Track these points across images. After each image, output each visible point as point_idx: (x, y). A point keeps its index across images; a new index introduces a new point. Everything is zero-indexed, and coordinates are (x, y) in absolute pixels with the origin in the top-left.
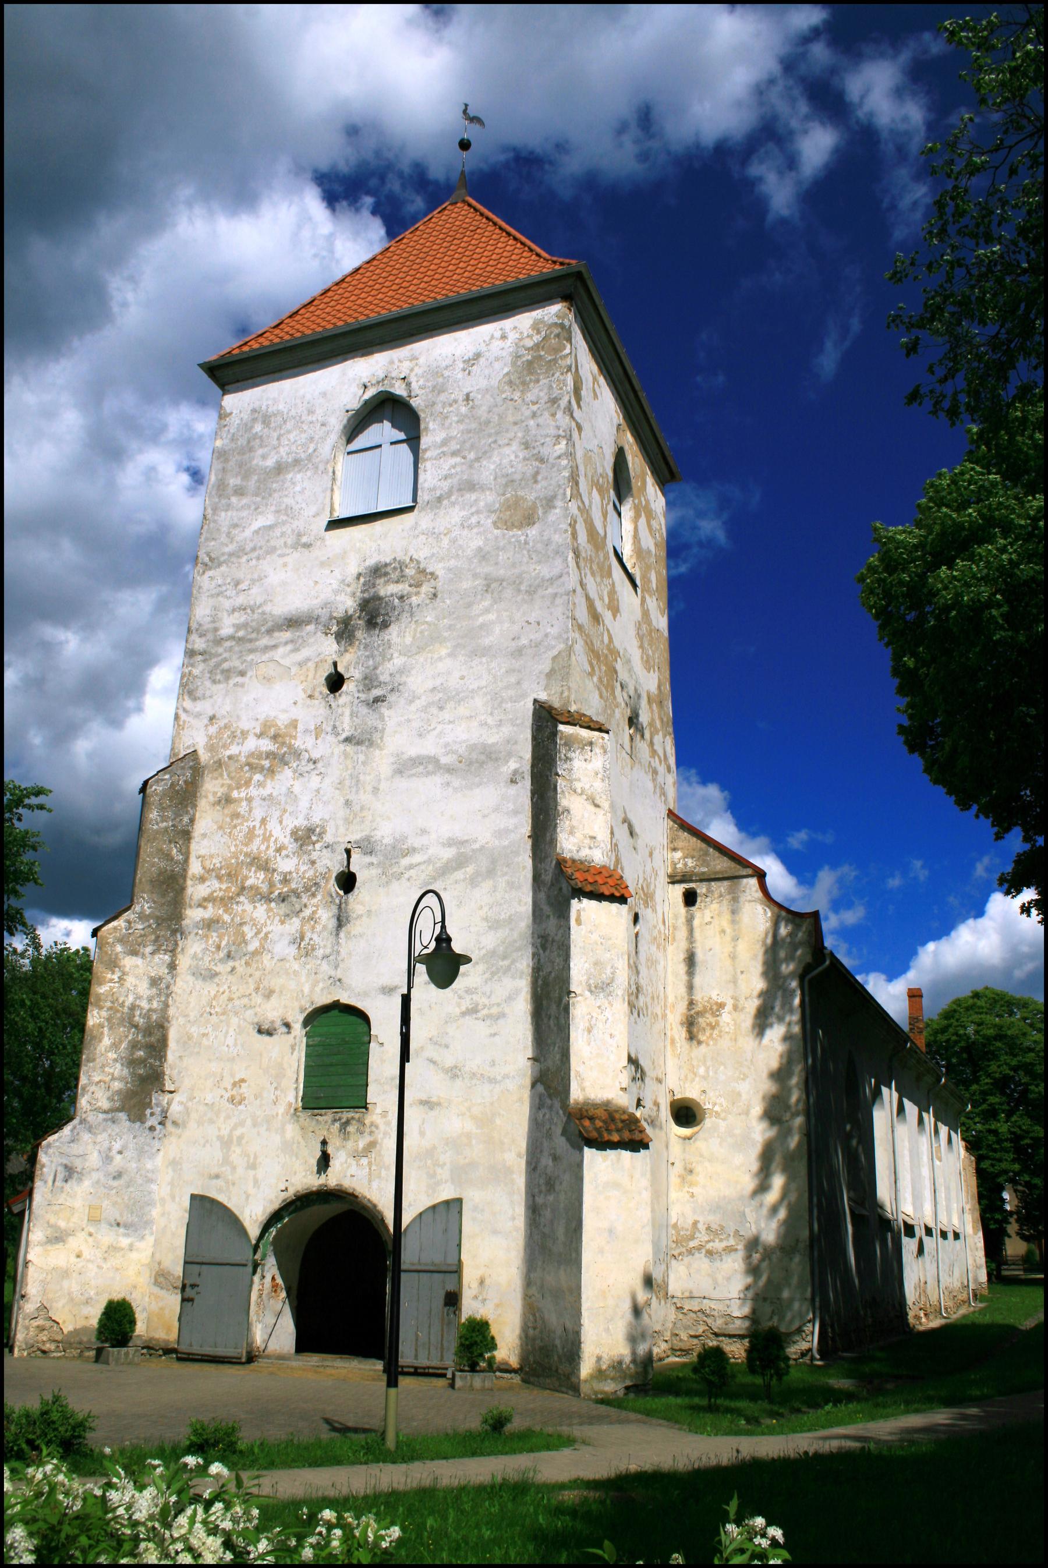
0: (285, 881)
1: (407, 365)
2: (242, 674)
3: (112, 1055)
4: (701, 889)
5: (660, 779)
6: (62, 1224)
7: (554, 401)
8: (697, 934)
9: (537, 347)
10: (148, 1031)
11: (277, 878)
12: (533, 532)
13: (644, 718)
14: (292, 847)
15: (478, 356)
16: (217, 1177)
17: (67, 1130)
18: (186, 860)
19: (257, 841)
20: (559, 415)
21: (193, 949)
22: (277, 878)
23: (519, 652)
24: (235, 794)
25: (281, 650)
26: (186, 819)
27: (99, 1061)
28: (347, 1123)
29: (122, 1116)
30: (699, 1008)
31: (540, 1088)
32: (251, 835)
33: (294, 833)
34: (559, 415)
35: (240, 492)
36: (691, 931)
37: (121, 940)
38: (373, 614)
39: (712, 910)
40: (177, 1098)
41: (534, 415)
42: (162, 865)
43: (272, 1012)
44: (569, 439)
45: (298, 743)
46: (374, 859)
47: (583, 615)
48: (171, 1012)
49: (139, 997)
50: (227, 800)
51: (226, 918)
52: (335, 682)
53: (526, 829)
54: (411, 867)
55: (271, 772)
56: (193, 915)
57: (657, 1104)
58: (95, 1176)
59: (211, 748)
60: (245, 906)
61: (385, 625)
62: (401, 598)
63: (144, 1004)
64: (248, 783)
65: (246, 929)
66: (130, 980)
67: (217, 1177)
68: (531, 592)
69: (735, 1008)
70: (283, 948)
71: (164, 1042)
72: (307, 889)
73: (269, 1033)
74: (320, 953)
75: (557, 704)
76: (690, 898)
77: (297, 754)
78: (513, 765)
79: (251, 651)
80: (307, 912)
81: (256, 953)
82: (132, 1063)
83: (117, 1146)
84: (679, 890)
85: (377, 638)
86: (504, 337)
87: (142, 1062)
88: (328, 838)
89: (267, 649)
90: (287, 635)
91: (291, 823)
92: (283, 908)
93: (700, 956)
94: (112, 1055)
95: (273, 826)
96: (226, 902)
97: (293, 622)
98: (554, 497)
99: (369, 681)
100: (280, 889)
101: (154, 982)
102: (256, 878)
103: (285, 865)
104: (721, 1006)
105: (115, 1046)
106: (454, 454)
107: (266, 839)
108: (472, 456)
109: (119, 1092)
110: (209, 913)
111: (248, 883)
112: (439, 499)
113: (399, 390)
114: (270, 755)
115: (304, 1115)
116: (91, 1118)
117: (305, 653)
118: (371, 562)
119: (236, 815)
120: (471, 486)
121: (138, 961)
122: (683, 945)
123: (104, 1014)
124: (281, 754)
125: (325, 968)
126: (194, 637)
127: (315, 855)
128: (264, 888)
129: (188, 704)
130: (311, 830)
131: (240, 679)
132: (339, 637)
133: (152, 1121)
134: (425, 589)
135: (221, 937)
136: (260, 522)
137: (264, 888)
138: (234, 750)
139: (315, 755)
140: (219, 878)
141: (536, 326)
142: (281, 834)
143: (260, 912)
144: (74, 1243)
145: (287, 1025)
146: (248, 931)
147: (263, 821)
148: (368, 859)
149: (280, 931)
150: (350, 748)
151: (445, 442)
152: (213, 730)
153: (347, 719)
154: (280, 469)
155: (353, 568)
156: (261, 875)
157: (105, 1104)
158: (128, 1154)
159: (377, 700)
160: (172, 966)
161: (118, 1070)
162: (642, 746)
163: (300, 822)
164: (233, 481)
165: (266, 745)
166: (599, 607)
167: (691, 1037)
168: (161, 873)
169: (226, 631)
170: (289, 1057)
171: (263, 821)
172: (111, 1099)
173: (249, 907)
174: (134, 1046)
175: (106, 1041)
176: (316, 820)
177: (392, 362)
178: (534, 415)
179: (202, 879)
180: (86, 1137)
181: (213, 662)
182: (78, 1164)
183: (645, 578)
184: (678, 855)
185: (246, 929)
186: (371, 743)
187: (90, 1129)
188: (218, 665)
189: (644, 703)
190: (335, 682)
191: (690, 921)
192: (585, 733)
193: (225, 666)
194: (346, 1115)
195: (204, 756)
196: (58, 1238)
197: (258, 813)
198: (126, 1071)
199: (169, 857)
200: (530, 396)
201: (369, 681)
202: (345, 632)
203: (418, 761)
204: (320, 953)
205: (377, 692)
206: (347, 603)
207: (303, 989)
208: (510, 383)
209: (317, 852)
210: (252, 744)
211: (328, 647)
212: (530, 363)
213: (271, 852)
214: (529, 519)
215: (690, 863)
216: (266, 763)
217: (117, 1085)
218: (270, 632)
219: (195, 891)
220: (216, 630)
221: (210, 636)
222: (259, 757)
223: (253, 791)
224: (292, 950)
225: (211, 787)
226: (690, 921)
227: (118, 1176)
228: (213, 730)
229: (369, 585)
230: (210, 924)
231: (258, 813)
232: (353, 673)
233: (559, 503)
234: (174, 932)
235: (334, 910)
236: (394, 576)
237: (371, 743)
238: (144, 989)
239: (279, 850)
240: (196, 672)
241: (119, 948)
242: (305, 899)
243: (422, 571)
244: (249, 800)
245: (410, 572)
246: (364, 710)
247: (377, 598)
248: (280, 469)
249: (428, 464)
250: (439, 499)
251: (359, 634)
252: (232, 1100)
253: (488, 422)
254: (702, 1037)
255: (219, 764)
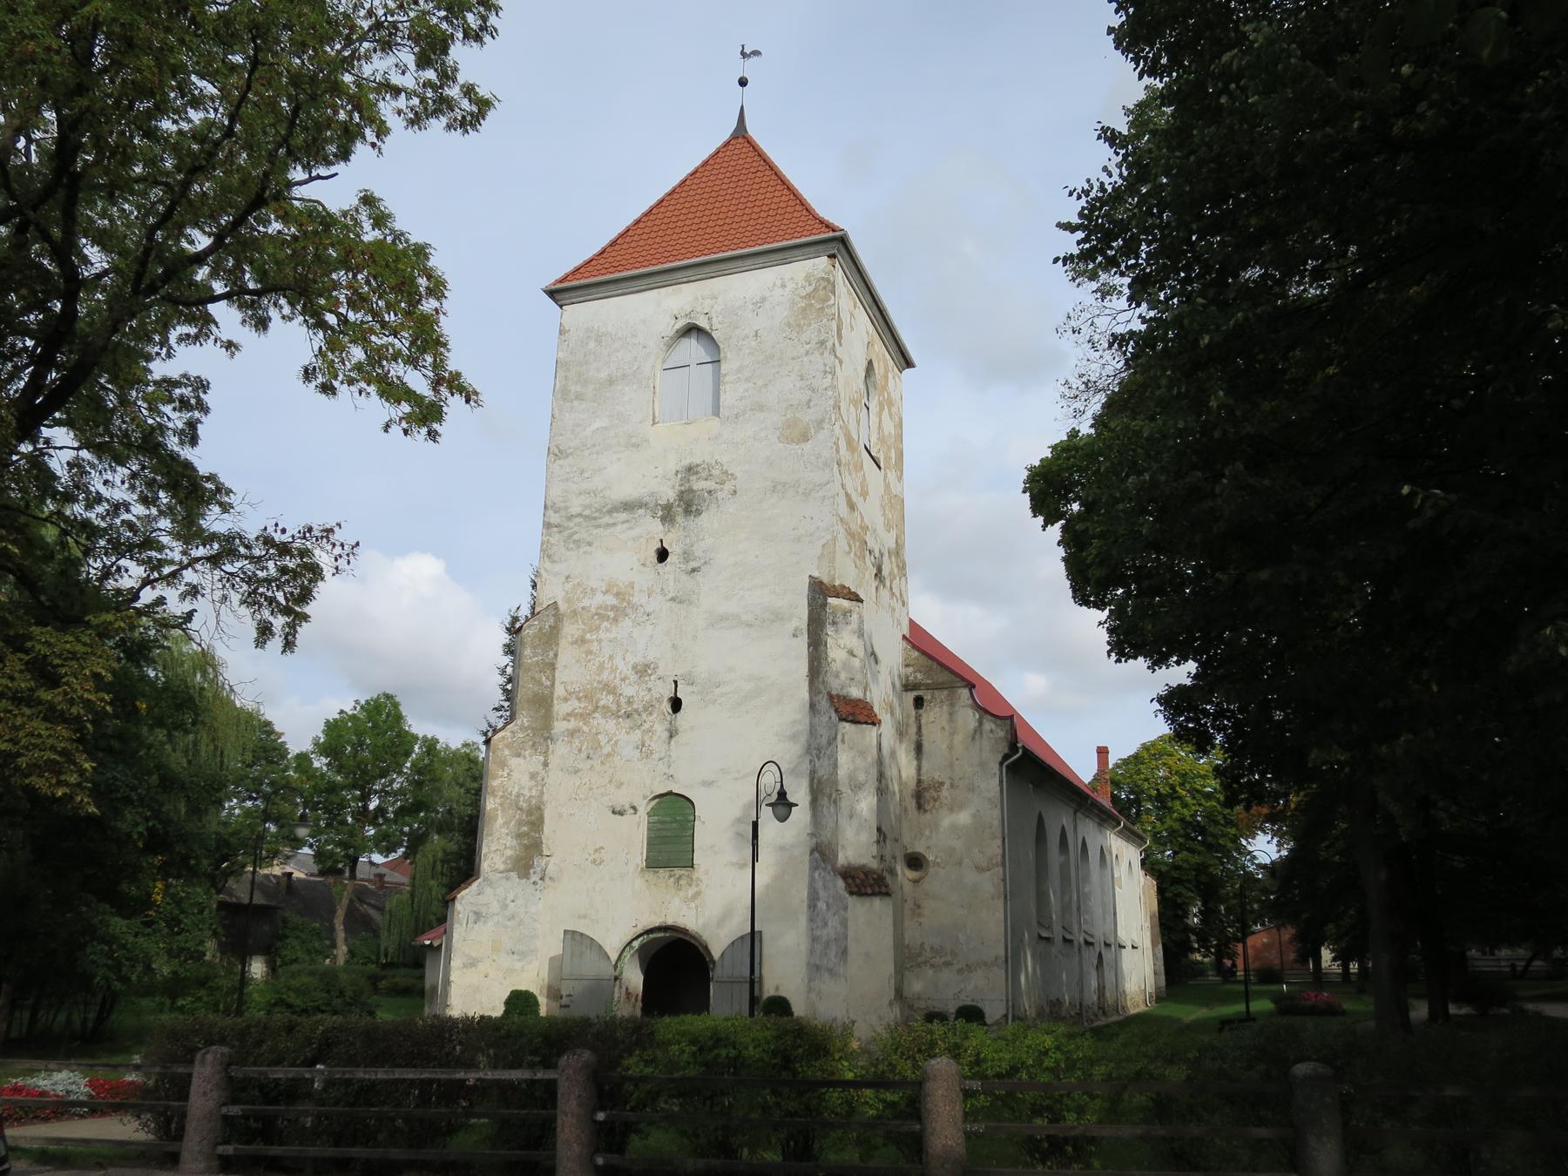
0: (629, 703)
1: (708, 302)
2: (590, 544)
3: (505, 831)
4: (927, 696)
5: (897, 614)
6: (474, 954)
7: (822, 343)
8: (924, 731)
9: (808, 296)
10: (530, 813)
11: (623, 700)
12: (807, 446)
13: (885, 572)
14: (633, 677)
15: (763, 300)
16: (585, 917)
17: (475, 885)
18: (553, 685)
19: (606, 673)
20: (826, 354)
21: (561, 751)
22: (623, 700)
23: (798, 539)
24: (588, 636)
25: (619, 527)
26: (551, 654)
27: (496, 835)
28: (680, 877)
29: (514, 875)
30: (925, 785)
31: (817, 855)
32: (601, 667)
33: (634, 668)
34: (826, 354)
35: (579, 397)
36: (919, 728)
37: (508, 746)
38: (688, 504)
39: (934, 716)
40: (552, 860)
41: (807, 353)
42: (536, 689)
43: (622, 798)
44: (833, 373)
45: (634, 600)
46: (694, 689)
47: (843, 510)
48: (545, 798)
49: (522, 788)
50: (582, 641)
51: (585, 729)
52: (663, 555)
53: (804, 670)
54: (722, 695)
55: (616, 620)
56: (559, 727)
57: (894, 857)
58: (496, 918)
59: (568, 601)
60: (598, 720)
61: (699, 513)
62: (710, 492)
63: (526, 792)
64: (598, 628)
65: (600, 737)
66: (515, 775)
67: (585, 917)
68: (807, 494)
69: (952, 786)
70: (628, 751)
71: (541, 819)
72: (645, 709)
73: (621, 813)
74: (657, 756)
75: (825, 580)
76: (919, 702)
77: (635, 608)
78: (795, 623)
79: (599, 526)
80: (646, 726)
81: (608, 755)
82: (519, 836)
83: (511, 897)
84: (911, 696)
85: (692, 522)
86: (783, 286)
87: (525, 834)
88: (660, 672)
89: (608, 525)
90: (623, 516)
91: (631, 660)
92: (628, 723)
93: (926, 746)
94: (505, 831)
95: (618, 661)
96: (584, 717)
97: (628, 506)
98: (823, 421)
99: (687, 556)
100: (625, 708)
101: (533, 776)
102: (606, 700)
103: (628, 690)
104: (942, 784)
105: (506, 823)
106: (747, 380)
107: (614, 670)
108: (760, 383)
109: (510, 857)
110: (572, 724)
111: (601, 703)
112: (737, 416)
113: (702, 323)
114: (613, 608)
115: (650, 875)
116: (494, 877)
117: (637, 531)
118: (686, 463)
119: (589, 652)
120: (761, 408)
121: (520, 760)
122: (914, 737)
123: (498, 800)
124: (621, 607)
125: (661, 767)
126: (550, 512)
127: (650, 685)
128: (614, 707)
129: (548, 565)
130: (647, 666)
131: (588, 548)
132: (663, 519)
133: (534, 878)
134: (728, 486)
135: (581, 742)
136: (598, 424)
137: (614, 707)
138: (586, 603)
139: (649, 610)
140: (579, 699)
141: (808, 278)
142: (624, 667)
143: (610, 725)
144: (481, 967)
145: (634, 808)
146: (602, 739)
147: (611, 658)
148: (690, 689)
149: (625, 739)
150: (673, 605)
151: (739, 370)
152: (568, 586)
153: (671, 583)
154: (611, 382)
155: (673, 464)
156: (611, 698)
157: (502, 867)
158: (519, 902)
159: (694, 570)
160: (546, 764)
161: (510, 841)
162: (885, 593)
163: (639, 659)
164: (574, 388)
165: (611, 600)
166: (854, 499)
167: (920, 807)
168: (536, 695)
169: (574, 510)
170: (635, 833)
171: (611, 658)
172: (505, 862)
173: (602, 721)
174: (520, 823)
175: (500, 821)
176: (651, 658)
177: (696, 299)
178: (807, 353)
179: (566, 700)
180: (488, 890)
181: (566, 534)
182: (484, 910)
183: (888, 458)
184: (910, 670)
185: (600, 737)
186: (690, 603)
187: (491, 885)
188: (570, 536)
189: (886, 558)
190: (663, 555)
191: (918, 718)
192: (845, 603)
193: (576, 537)
194: (678, 872)
195: (563, 607)
196: (472, 963)
197: (607, 652)
198: (515, 842)
199: (540, 683)
200: (804, 337)
201: (687, 556)
202: (667, 516)
203: (724, 618)
204: (657, 756)
205: (694, 564)
206: (669, 494)
207: (642, 783)
208: (789, 325)
209: (652, 681)
210: (600, 599)
211: (652, 530)
212: (804, 309)
213: (617, 681)
214: (805, 437)
215: (919, 676)
216: (612, 614)
217: (509, 852)
218: (610, 512)
219: (560, 708)
220: (566, 508)
221: (563, 513)
222: (606, 608)
223: (602, 635)
224: (637, 754)
225: (570, 630)
226: (918, 718)
227: (512, 917)
228: (568, 586)
229: (686, 480)
230: (572, 733)
231: (607, 652)
232: (674, 550)
233: (826, 426)
234: (546, 739)
235: (667, 725)
236: (704, 475)
237: (690, 603)
238: (526, 781)
239: (623, 680)
240: (552, 540)
241: (507, 752)
242: (644, 716)
243: (726, 472)
244: (599, 641)
245: (716, 472)
246: (684, 577)
247: (691, 490)
248: (611, 382)
249: (727, 387)
250: (737, 416)
251: (680, 519)
252: (594, 861)
253: (772, 357)
254: (927, 807)
255: (575, 613)
